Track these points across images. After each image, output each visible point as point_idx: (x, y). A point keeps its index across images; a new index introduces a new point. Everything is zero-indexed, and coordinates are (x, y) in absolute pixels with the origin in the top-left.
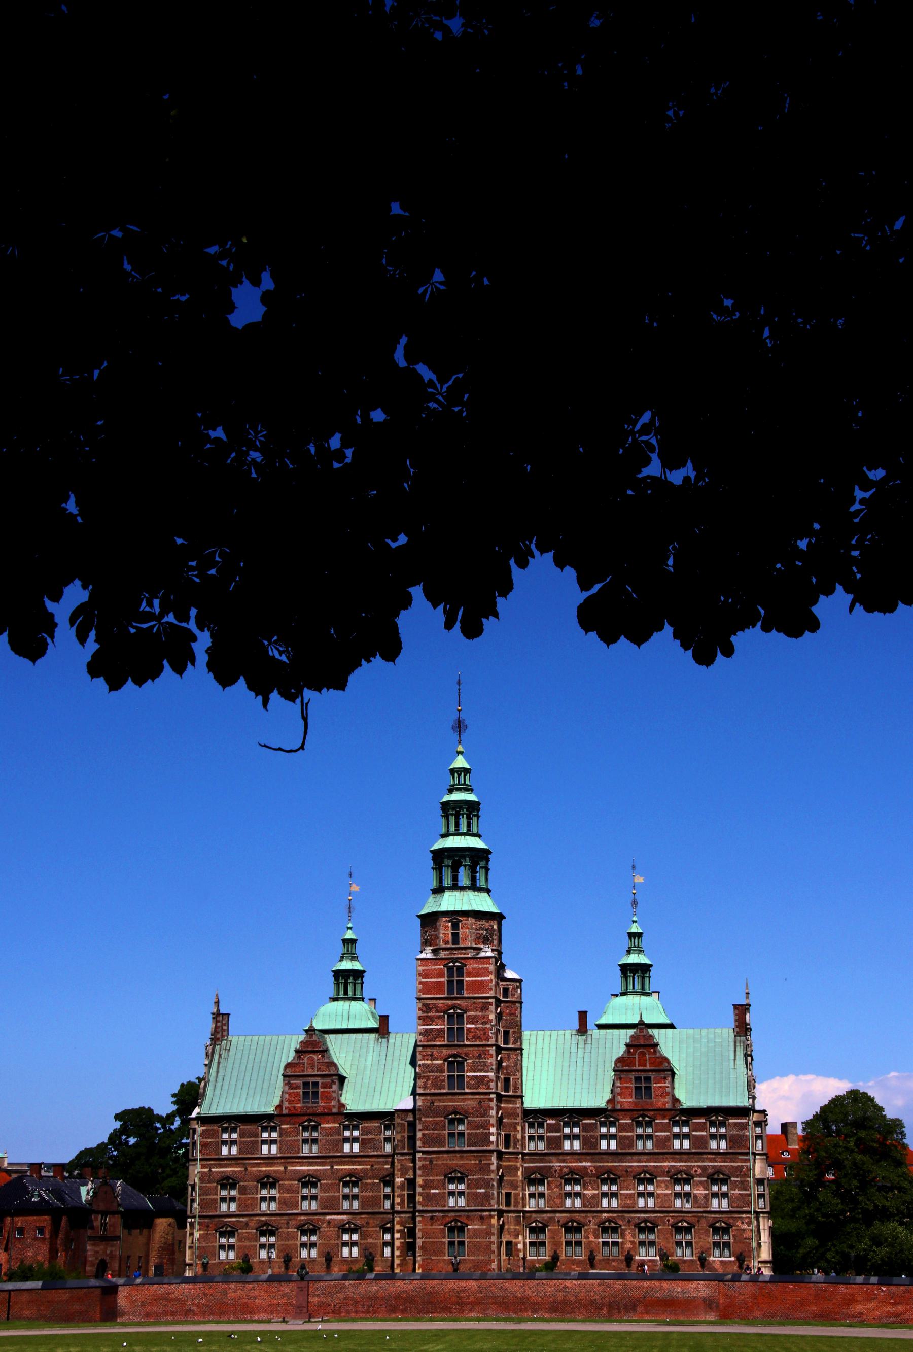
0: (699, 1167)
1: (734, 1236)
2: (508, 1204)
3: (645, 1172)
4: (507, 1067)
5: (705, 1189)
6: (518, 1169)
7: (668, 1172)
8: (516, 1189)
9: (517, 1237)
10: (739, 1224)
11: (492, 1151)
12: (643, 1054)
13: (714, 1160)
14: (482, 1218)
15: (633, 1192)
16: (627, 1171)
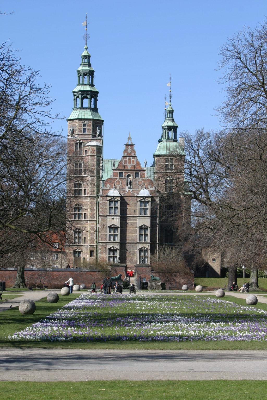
8: (87, 236)
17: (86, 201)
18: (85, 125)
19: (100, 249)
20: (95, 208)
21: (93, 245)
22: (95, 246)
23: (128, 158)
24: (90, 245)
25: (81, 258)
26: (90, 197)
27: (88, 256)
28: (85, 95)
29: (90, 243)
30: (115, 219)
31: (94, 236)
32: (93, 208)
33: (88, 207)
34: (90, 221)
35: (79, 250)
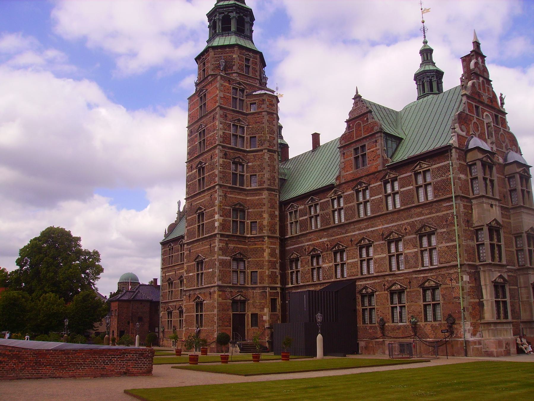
0: (408, 224)
1: (443, 296)
2: (254, 282)
3: (363, 239)
4: (253, 166)
5: (415, 246)
6: (264, 251)
7: (383, 235)
9: (263, 308)
10: (447, 281)
11: (216, 234)
12: (359, 125)
13: (421, 214)
14: (210, 294)
15: (356, 260)
16: (351, 241)
17: (257, 197)
18: (247, 60)
19: (469, 283)
20: (277, 213)
21: (275, 288)
22: (279, 290)
23: (481, 79)
24: (272, 288)
25: (245, 314)
26: (268, 189)
27: (266, 310)
28: (242, 15)
29: (271, 283)
30: (494, 207)
31: (276, 269)
32: (274, 212)
33: (265, 208)
34: (269, 237)
35: (243, 298)
